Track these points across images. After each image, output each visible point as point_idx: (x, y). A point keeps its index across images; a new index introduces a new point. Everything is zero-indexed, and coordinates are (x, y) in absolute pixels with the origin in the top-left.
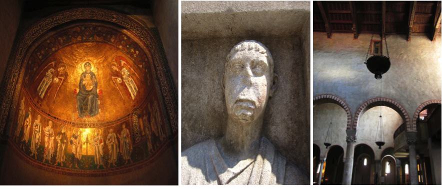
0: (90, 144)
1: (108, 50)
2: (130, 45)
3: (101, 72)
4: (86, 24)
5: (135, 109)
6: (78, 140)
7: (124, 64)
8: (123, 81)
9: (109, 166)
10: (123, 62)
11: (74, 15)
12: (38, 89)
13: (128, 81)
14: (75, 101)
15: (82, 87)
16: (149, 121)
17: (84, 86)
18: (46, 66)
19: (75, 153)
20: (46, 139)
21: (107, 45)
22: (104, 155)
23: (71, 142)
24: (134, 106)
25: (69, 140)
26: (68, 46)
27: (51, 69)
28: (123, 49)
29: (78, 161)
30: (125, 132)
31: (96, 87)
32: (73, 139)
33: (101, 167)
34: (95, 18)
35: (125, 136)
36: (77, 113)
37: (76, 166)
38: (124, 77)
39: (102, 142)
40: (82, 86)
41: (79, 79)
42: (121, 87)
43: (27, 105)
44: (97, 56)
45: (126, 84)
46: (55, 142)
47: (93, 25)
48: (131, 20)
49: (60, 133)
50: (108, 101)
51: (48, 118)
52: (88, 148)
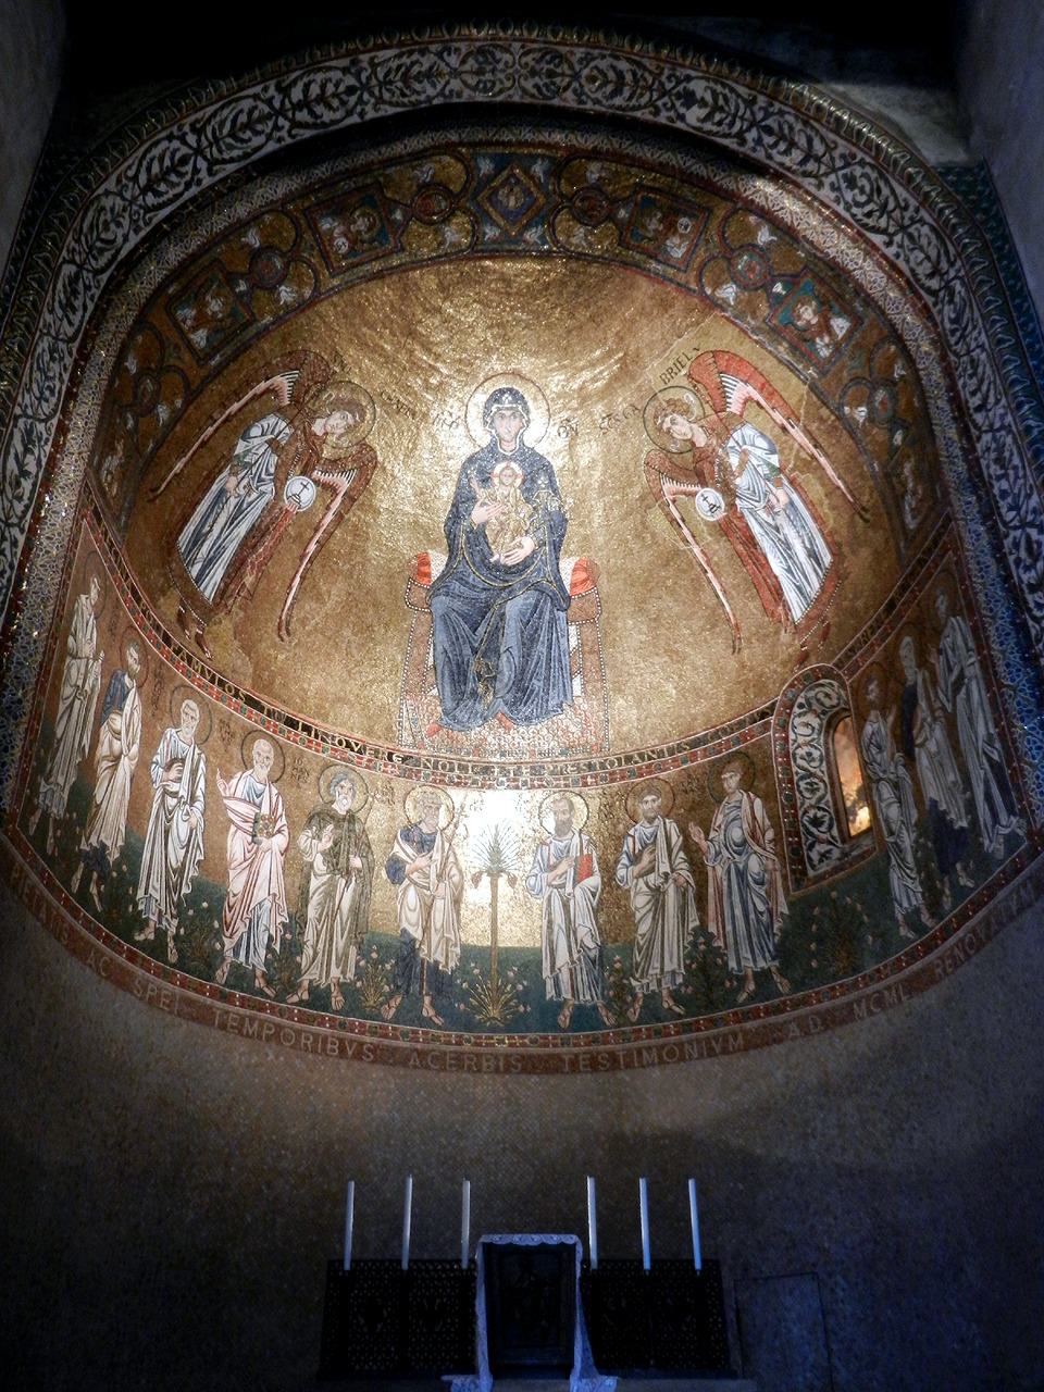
0: (512, 881)
1: (642, 312)
2: (792, 282)
3: (589, 451)
4: (507, 136)
5: (811, 679)
6: (437, 855)
7: (748, 400)
8: (732, 506)
9: (634, 1014)
10: (738, 392)
11: (430, 75)
12: (184, 539)
13: (769, 508)
14: (422, 630)
15: (463, 539)
16: (906, 743)
17: (478, 536)
18: (238, 396)
19: (417, 934)
20: (236, 845)
21: (643, 282)
22: (601, 948)
23: (396, 871)
24: (803, 659)
25: (378, 855)
26: (379, 276)
27: (272, 420)
28: (745, 309)
29: (439, 982)
30: (741, 811)
31: (556, 547)
32: (403, 851)
33: (584, 1017)
34: (569, 100)
35: (736, 834)
36: (431, 703)
37: (428, 1011)
38: (742, 482)
39: (590, 874)
40: (463, 539)
41: (447, 492)
42: (721, 549)
43: (114, 635)
44: (566, 351)
45: (756, 529)
46: (294, 864)
47: (556, 146)
48: (811, 116)
49: (320, 817)
50: (631, 631)
51: (247, 719)
52: (502, 907)
